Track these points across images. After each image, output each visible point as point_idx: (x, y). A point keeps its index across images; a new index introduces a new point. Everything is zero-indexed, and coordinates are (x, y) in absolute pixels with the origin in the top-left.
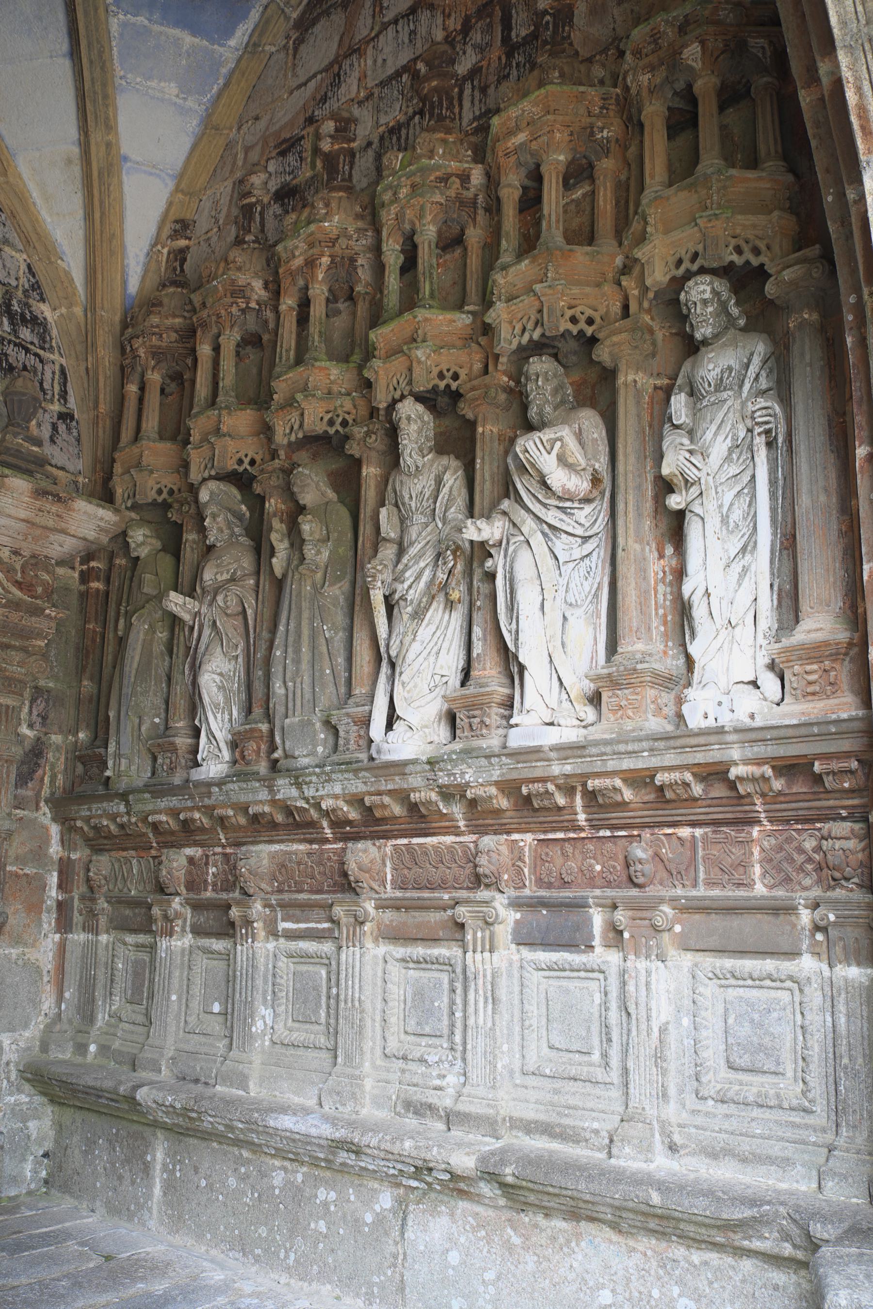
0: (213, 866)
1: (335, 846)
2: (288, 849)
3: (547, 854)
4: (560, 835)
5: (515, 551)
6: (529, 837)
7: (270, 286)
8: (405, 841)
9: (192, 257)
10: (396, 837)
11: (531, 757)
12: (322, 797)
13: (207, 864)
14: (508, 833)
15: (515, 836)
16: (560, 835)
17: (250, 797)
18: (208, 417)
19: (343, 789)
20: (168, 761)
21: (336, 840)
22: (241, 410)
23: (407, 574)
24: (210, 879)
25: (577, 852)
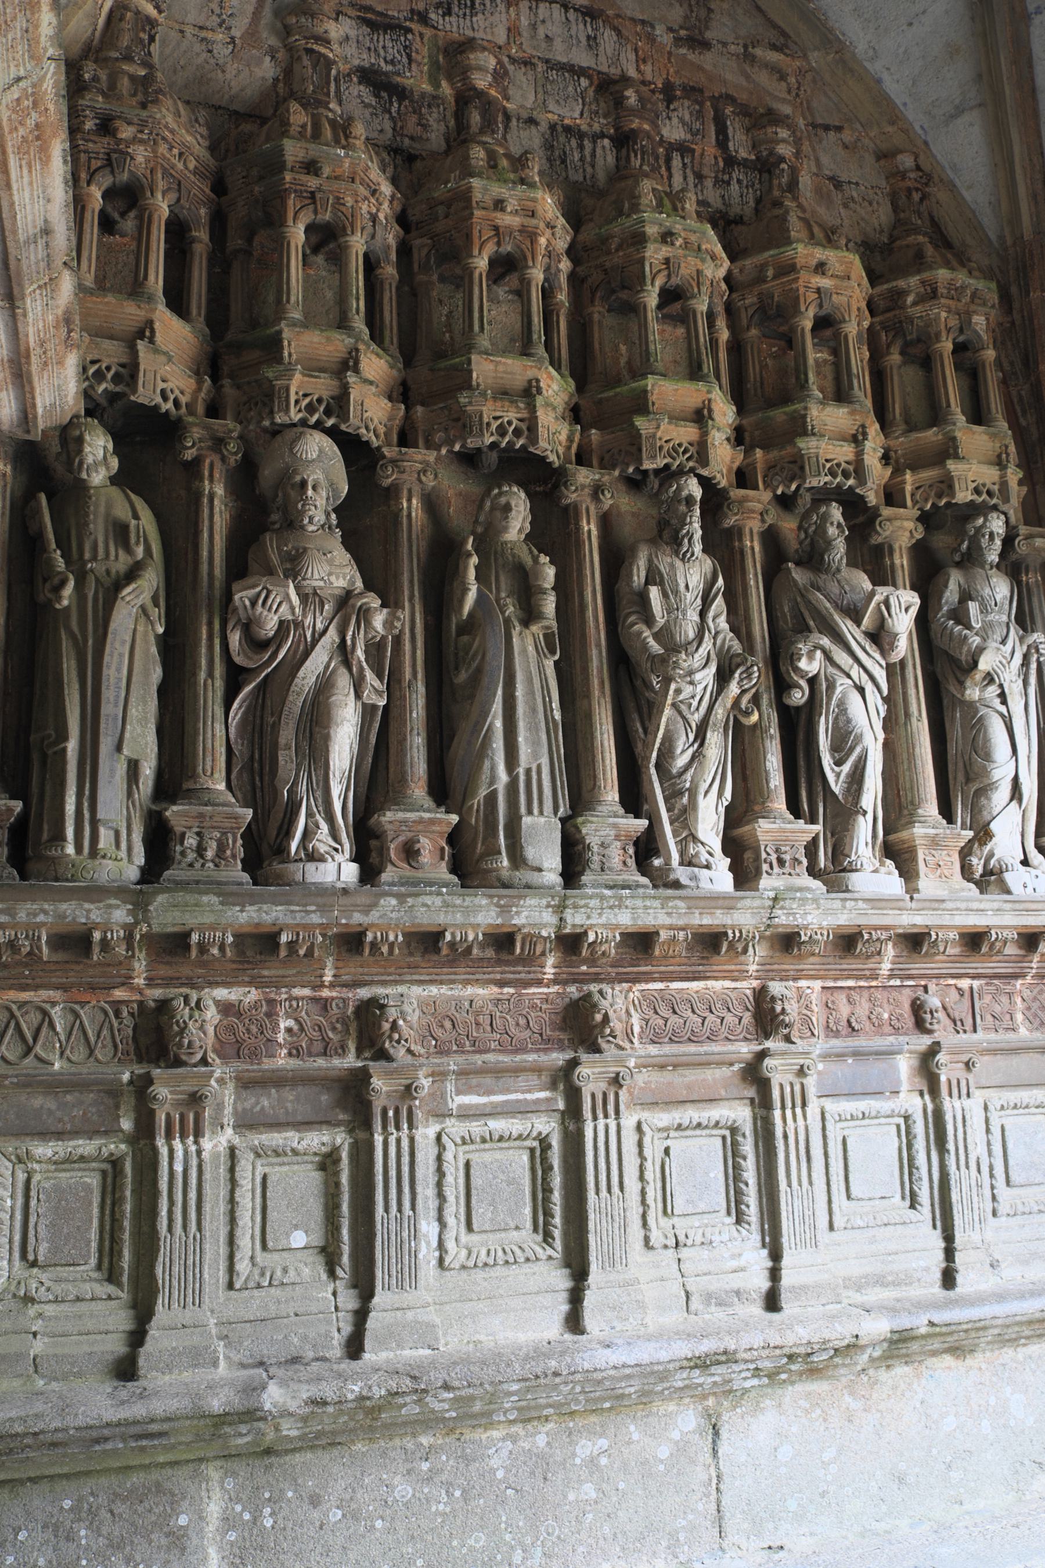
0: (288, 1016)
1: (545, 990)
2: (456, 993)
3: (833, 1002)
4: (851, 983)
5: (844, 694)
6: (817, 984)
7: (395, 202)
8: (659, 986)
9: (163, 42)
10: (647, 981)
11: (883, 904)
12: (592, 926)
13: (271, 1015)
14: (795, 979)
15: (803, 983)
16: (851, 983)
17: (459, 918)
18: (328, 339)
19: (633, 919)
20: (214, 845)
21: (555, 982)
22: (377, 355)
23: (698, 676)
24: (281, 1037)
25: (863, 1000)
